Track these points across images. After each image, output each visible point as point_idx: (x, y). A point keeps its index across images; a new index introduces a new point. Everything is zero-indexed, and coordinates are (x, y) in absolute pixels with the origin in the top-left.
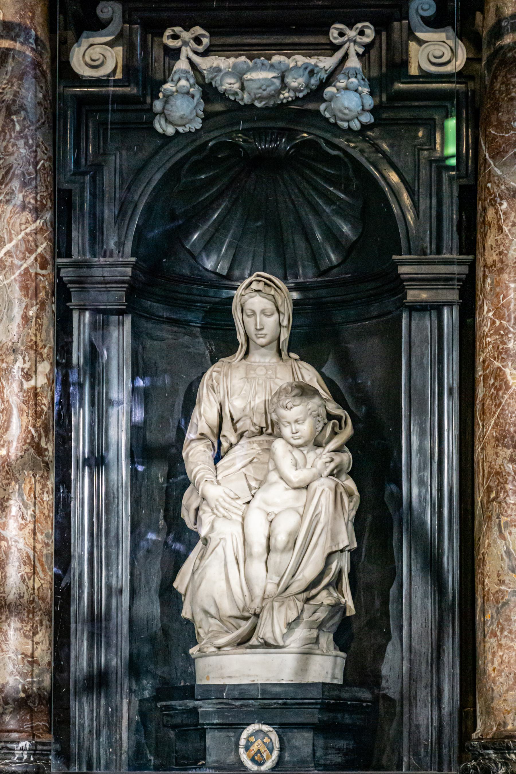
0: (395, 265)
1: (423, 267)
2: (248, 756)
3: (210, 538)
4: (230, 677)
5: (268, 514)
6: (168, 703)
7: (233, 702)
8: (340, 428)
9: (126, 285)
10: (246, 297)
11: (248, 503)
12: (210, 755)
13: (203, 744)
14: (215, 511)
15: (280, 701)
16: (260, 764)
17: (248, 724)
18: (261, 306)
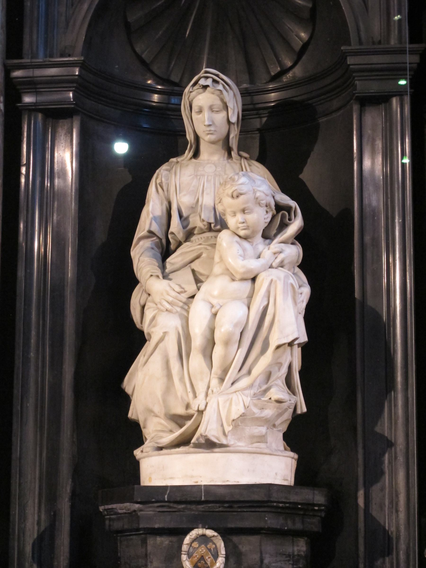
0: (344, 56)
1: (373, 57)
2: (191, 562)
3: (153, 332)
4: (171, 478)
5: (213, 306)
6: (110, 507)
7: (175, 506)
8: (290, 219)
10: (193, 93)
11: (193, 297)
12: (151, 562)
13: (144, 550)
14: (159, 306)
15: (226, 505)
17: (192, 529)
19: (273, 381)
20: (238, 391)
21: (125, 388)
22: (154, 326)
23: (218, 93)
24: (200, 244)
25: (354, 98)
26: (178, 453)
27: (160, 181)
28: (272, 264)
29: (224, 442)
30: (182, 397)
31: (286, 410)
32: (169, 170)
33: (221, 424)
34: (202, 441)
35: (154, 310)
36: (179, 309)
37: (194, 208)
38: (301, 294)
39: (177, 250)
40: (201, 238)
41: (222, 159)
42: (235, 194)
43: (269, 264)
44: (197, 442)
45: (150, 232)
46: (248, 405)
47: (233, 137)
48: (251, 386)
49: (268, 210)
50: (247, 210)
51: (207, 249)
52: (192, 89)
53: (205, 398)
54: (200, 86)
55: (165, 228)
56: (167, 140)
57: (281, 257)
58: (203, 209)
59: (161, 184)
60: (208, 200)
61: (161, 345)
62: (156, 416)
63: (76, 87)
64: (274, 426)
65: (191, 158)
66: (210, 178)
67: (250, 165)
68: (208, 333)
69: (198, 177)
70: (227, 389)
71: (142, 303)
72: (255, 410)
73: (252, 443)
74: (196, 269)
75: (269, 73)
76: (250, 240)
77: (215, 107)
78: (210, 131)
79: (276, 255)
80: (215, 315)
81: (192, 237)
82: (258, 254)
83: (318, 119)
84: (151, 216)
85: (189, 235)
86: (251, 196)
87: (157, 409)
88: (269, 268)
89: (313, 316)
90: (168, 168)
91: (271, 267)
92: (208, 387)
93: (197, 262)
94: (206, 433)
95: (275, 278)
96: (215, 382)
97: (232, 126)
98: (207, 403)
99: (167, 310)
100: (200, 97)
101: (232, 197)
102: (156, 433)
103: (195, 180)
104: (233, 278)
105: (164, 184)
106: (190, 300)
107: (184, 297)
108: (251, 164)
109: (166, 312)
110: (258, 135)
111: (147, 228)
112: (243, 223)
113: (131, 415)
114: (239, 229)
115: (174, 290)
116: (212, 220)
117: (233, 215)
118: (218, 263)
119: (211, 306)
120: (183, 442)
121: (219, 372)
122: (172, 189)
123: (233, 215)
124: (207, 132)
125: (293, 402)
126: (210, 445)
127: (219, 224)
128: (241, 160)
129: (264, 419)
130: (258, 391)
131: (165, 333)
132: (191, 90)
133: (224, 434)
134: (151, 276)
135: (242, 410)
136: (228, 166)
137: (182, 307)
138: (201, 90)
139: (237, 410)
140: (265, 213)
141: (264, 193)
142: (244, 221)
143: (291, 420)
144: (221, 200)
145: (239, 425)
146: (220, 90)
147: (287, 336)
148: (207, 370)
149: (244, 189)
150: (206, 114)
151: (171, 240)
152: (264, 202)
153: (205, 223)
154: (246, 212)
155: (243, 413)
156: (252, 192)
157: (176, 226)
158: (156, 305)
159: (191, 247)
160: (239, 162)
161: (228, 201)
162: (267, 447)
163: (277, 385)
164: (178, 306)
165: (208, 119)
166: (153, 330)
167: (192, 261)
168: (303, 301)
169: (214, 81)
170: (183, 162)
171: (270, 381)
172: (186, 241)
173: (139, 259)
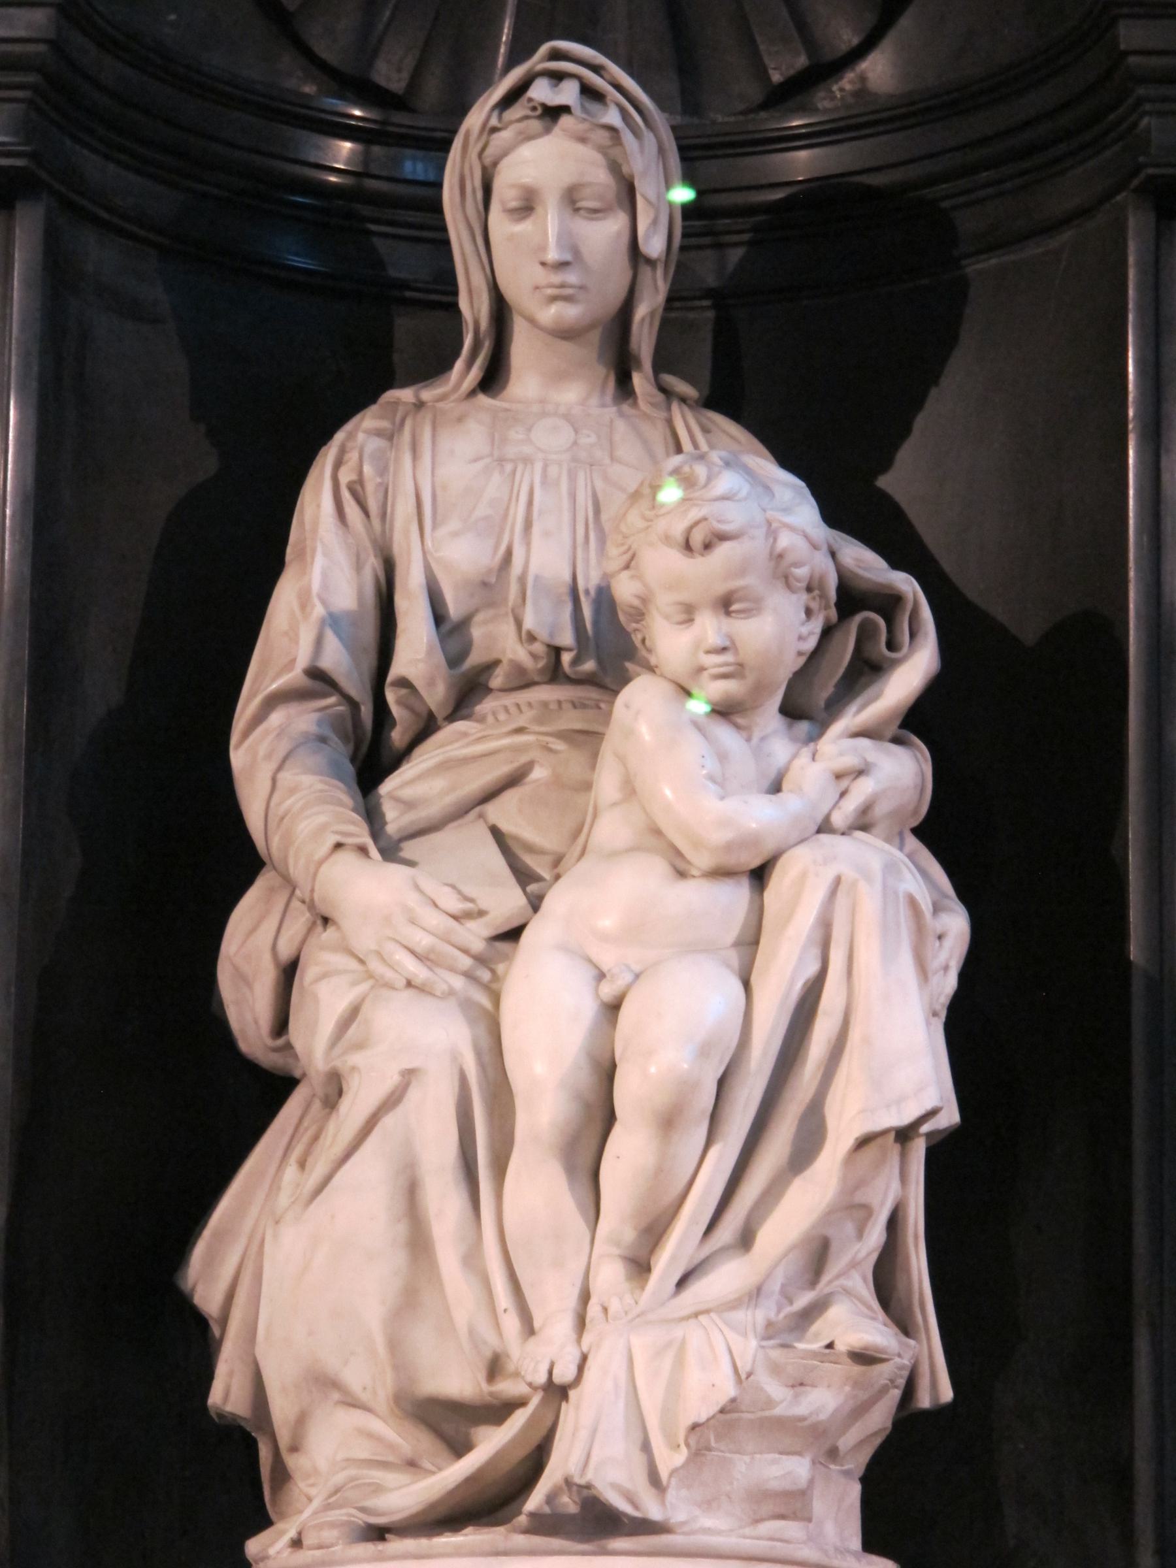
3: (354, 1069)
5: (601, 976)
8: (892, 645)
9: (31, 78)
10: (506, 135)
11: (513, 934)
14: (375, 965)
18: (556, 189)
19: (838, 1277)
20: (707, 1312)
21: (193, 1289)
22: (360, 1046)
23: (602, 137)
24: (520, 730)
25: (1135, 182)
26: (458, 1553)
27: (354, 477)
28: (827, 819)
29: (654, 1513)
30: (471, 1332)
31: (884, 1390)
32: (390, 436)
33: (639, 1443)
34: (569, 1504)
35: (354, 984)
36: (458, 983)
37: (491, 586)
38: (940, 937)
39: (418, 751)
40: (518, 706)
41: (594, 401)
42: (697, 538)
43: (819, 818)
44: (547, 1510)
45: (316, 674)
46: (748, 1368)
47: (643, 319)
48: (756, 1294)
49: (814, 605)
50: (740, 600)
51: (550, 750)
52: (500, 118)
53: (574, 1336)
54: (534, 109)
55: (369, 661)
56: (377, 314)
57: (863, 790)
58: (529, 593)
59: (359, 488)
60: (547, 558)
61: (388, 1121)
62: (353, 1403)
63: (34, 88)
64: (833, 1454)
65: (472, 393)
66: (553, 471)
67: (706, 430)
68: (586, 1079)
69: (509, 467)
70: (663, 1304)
71: (286, 951)
72: (775, 1389)
73: (757, 1521)
74: (505, 827)
75: (762, 73)
76: (740, 720)
77: (587, 191)
78: (562, 286)
79: (844, 783)
80: (613, 1008)
81: (480, 702)
82: (772, 774)
83: (964, 262)
84: (319, 611)
85: (469, 692)
86: (753, 546)
87: (357, 1376)
88: (819, 831)
90: (385, 424)
91: (825, 827)
92: (585, 1297)
93: (510, 798)
94: (590, 1476)
95: (849, 873)
96: (610, 1275)
97: (646, 272)
98: (584, 1358)
99: (409, 984)
100: (526, 151)
101: (688, 547)
102: (353, 1472)
103: (496, 478)
104: (682, 866)
105: (370, 488)
106: (502, 946)
107: (475, 935)
108: (710, 425)
109: (410, 992)
110: (711, 314)
111: (303, 659)
112: (724, 650)
113: (226, 1393)
114: (705, 674)
115: (436, 906)
116: (567, 638)
117: (683, 617)
118: (614, 804)
119: (594, 972)
120: (486, 1505)
121: (629, 1235)
122: (403, 509)
123: (683, 617)
124: (550, 291)
125: (906, 1362)
126: (596, 1521)
127: (600, 653)
128: (669, 409)
129: (806, 1423)
130: (782, 1315)
131: (409, 1075)
132: (494, 121)
133: (654, 1479)
134: (338, 846)
135: (729, 1390)
136: (621, 426)
137: (468, 975)
138: (535, 125)
139: (707, 1388)
140: (803, 616)
141: (806, 536)
142: (727, 643)
143: (888, 1432)
144: (633, 557)
145: (709, 1449)
146: (611, 129)
147: (900, 1101)
148: (577, 1224)
149: (733, 517)
150: (551, 219)
151: (395, 710)
152: (802, 572)
153: (538, 648)
154: (734, 607)
155: (733, 1400)
156: (764, 529)
157: (422, 655)
158: (362, 962)
159: (479, 740)
160: (664, 414)
161: (663, 565)
162: (810, 1539)
163: (847, 1292)
164: (452, 969)
165: (560, 237)
166: (356, 1059)
167: (490, 795)
168: (946, 968)
169: (589, 92)
170: (440, 405)
171: (825, 1278)
172: (452, 718)
173: (274, 781)
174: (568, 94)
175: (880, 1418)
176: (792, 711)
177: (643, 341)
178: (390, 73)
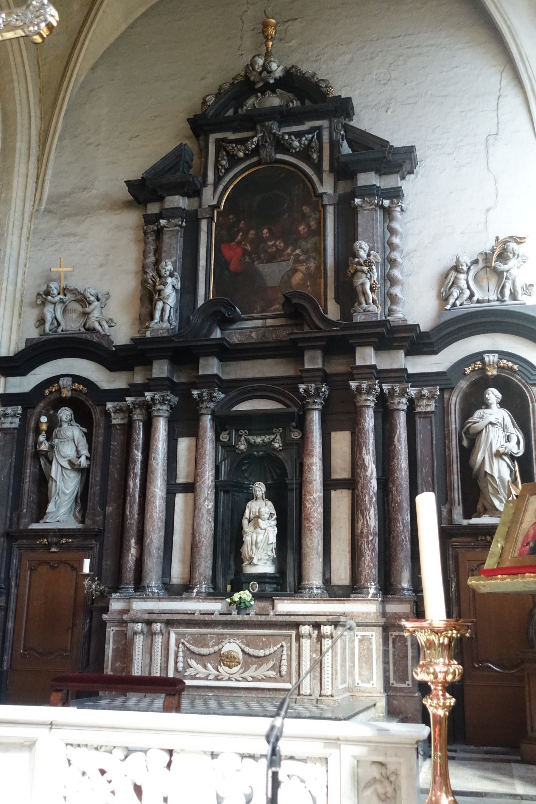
16: (254, 590)
89: (279, 537)
126: (255, 565)
174: (258, 485)
175: (272, 558)
176: (268, 519)
177: (264, 497)
178: (253, 481)
